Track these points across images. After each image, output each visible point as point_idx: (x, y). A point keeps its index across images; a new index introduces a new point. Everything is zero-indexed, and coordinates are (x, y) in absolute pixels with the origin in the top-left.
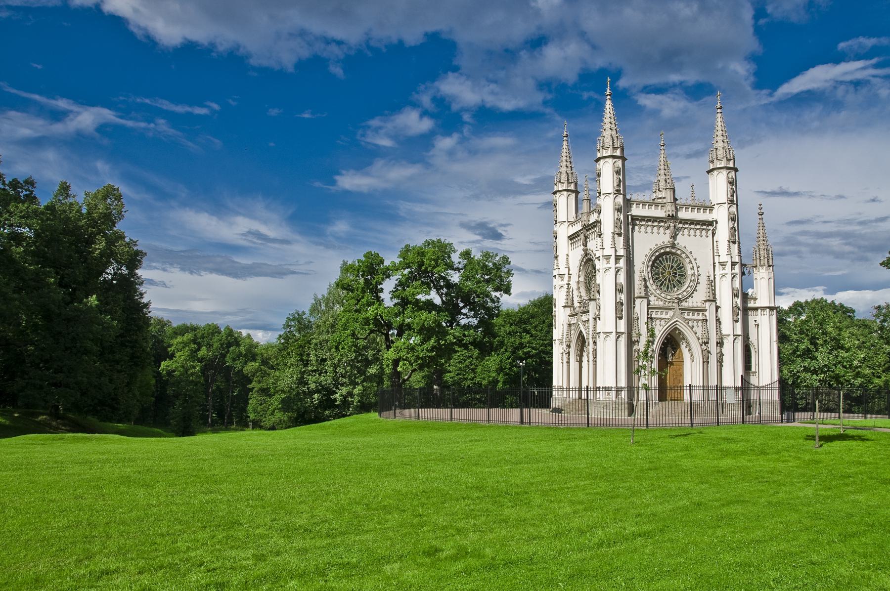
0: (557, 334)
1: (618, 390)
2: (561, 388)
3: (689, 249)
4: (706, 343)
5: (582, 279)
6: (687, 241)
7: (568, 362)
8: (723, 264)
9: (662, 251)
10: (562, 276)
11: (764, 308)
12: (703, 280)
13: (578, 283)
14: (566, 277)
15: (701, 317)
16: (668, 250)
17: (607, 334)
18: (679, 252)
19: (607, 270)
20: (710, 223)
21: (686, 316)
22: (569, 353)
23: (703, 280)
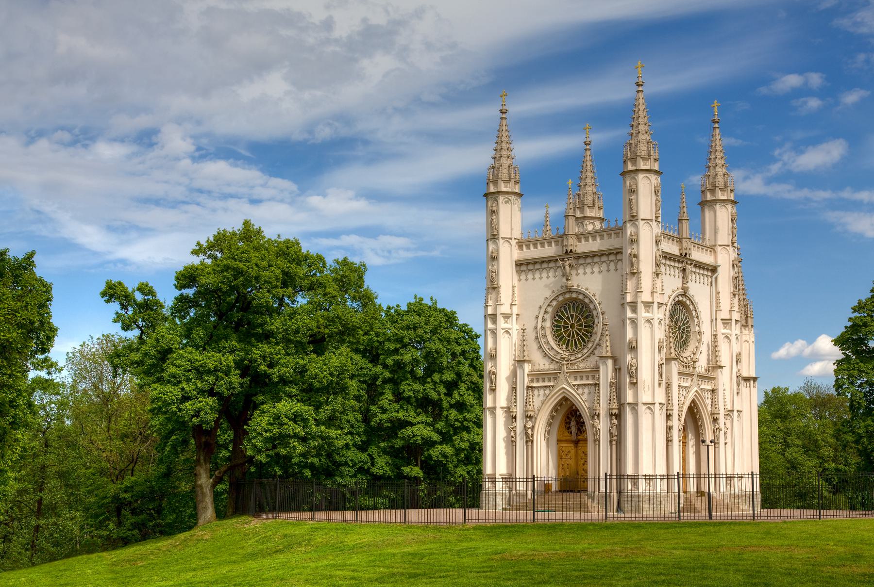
0: (498, 398)
1: (662, 477)
2: (510, 479)
3: (697, 299)
4: (715, 420)
5: (548, 324)
6: (699, 291)
7: (529, 440)
8: (726, 322)
9: (677, 299)
10: (507, 316)
11: (747, 379)
12: (707, 338)
13: (543, 328)
14: (514, 317)
15: (710, 387)
16: (680, 298)
17: (650, 405)
18: (688, 302)
19: (649, 321)
20: (714, 270)
21: (702, 386)
22: (533, 428)
23: (707, 338)
